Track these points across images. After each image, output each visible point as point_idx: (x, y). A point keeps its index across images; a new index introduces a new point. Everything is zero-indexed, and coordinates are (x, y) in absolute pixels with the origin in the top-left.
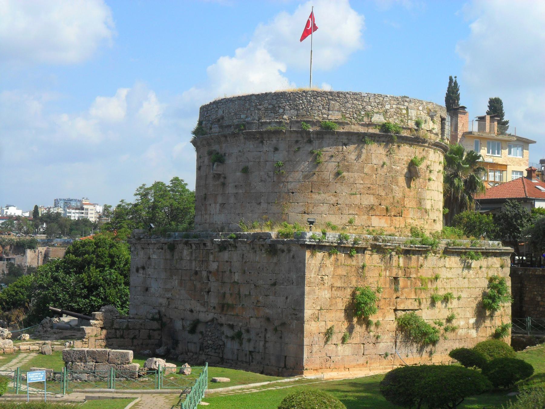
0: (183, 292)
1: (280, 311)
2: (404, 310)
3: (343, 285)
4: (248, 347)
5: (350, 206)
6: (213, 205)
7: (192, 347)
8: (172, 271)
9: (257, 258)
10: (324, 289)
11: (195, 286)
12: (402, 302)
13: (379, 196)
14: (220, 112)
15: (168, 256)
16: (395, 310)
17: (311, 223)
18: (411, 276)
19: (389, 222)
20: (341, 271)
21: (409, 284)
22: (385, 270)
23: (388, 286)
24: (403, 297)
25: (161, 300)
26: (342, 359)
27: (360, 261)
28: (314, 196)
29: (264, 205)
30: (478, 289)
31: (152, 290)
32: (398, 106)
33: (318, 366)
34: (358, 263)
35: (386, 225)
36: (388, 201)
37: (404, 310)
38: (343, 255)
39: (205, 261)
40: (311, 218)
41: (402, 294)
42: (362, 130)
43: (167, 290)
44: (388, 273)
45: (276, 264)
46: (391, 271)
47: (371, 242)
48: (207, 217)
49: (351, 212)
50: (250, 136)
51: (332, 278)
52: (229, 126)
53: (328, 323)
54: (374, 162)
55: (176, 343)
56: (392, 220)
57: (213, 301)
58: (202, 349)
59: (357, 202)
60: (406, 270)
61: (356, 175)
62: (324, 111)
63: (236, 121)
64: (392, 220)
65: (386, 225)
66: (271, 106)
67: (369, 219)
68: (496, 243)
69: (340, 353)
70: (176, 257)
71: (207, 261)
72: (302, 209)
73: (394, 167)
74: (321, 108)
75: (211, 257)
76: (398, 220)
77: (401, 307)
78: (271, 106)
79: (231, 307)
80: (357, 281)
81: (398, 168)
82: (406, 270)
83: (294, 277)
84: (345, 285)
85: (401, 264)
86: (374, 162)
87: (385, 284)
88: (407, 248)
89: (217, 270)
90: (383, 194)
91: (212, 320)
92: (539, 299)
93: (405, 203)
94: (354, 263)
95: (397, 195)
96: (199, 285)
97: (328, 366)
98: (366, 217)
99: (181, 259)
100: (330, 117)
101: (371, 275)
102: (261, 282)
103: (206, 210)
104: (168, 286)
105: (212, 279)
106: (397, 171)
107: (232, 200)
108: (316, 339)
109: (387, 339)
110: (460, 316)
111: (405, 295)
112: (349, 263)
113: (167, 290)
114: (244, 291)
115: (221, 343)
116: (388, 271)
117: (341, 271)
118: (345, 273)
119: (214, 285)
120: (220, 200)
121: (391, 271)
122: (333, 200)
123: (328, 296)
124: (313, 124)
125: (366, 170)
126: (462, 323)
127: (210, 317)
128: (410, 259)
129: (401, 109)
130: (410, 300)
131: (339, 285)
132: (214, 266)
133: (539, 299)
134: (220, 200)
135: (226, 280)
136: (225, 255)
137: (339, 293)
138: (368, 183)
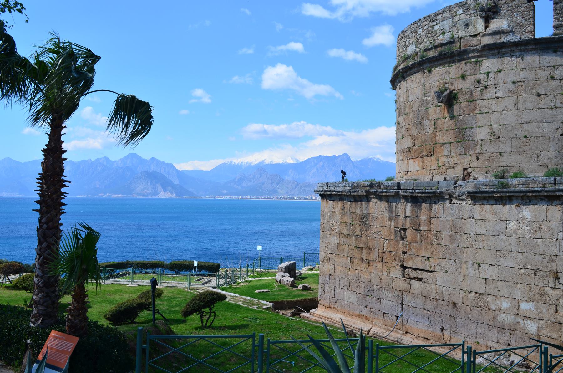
2: (415, 269)
3: (348, 233)
10: (334, 235)
13: (413, 137)
16: (404, 267)
18: (421, 228)
19: (421, 164)
20: (347, 219)
21: (419, 237)
22: (390, 219)
24: (411, 253)
26: (347, 304)
27: (364, 209)
30: (540, 258)
32: (431, 24)
34: (362, 211)
36: (420, 140)
37: (415, 269)
38: (349, 203)
41: (410, 249)
44: (393, 224)
47: (367, 189)
51: (340, 225)
53: (336, 267)
56: (423, 162)
64: (423, 162)
69: (346, 298)
73: (425, 98)
76: (429, 160)
80: (361, 230)
81: (429, 98)
84: (351, 233)
85: (408, 214)
87: (390, 235)
88: (407, 194)
93: (437, 139)
94: (358, 211)
95: (428, 130)
97: (335, 306)
101: (375, 224)
108: (327, 279)
109: (392, 297)
110: (501, 293)
112: (354, 211)
116: (393, 221)
118: (349, 221)
123: (337, 241)
128: (420, 208)
129: (433, 26)
130: (421, 258)
137: (345, 240)
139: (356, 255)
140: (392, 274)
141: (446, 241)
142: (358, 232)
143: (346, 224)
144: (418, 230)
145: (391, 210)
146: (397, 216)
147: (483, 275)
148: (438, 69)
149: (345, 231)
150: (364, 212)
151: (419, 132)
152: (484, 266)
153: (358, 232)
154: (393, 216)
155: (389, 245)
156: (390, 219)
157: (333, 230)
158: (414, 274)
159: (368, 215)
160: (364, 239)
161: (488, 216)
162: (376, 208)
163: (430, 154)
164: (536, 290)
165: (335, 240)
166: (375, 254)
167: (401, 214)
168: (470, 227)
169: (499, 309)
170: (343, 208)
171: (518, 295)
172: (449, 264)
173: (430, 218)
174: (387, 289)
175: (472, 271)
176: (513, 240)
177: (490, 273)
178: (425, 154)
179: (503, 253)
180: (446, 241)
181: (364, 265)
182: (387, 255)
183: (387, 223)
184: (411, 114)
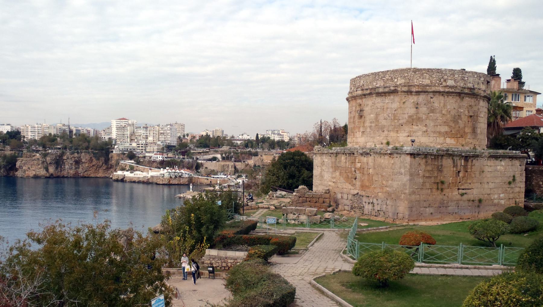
0: (342, 179)
1: (394, 189)
2: (463, 189)
4: (377, 208)
5: (434, 132)
6: (358, 133)
7: (346, 208)
8: (336, 168)
9: (382, 161)
11: (348, 176)
12: (462, 185)
14: (362, 82)
15: (333, 160)
17: (413, 142)
20: (429, 168)
23: (455, 176)
25: (330, 183)
28: (414, 127)
29: (386, 132)
31: (325, 178)
33: (415, 219)
35: (454, 143)
37: (463, 189)
39: (354, 163)
40: (413, 138)
42: (442, 90)
43: (334, 178)
45: (393, 164)
46: (457, 168)
48: (355, 139)
49: (434, 135)
50: (379, 94)
52: (367, 89)
54: (449, 107)
55: (337, 205)
56: (458, 140)
57: (358, 183)
58: (352, 209)
59: (438, 130)
60: (465, 167)
61: (438, 115)
62: (420, 80)
63: (370, 87)
64: (458, 140)
65: (454, 143)
66: (390, 78)
67: (445, 139)
68: (518, 152)
70: (338, 160)
71: (355, 162)
72: (407, 134)
74: (418, 78)
75: (357, 161)
77: (462, 187)
78: (390, 78)
79: (368, 187)
80: (437, 174)
82: (465, 167)
83: (403, 171)
85: (463, 164)
86: (449, 107)
89: (360, 167)
90: (453, 125)
91: (358, 193)
92: (541, 183)
94: (436, 163)
96: (350, 175)
98: (443, 138)
99: (340, 161)
100: (423, 83)
102: (384, 174)
103: (354, 135)
104: (334, 176)
105: (357, 172)
106: (461, 112)
107: (368, 130)
111: (464, 181)
113: (334, 178)
114: (375, 178)
115: (362, 206)
117: (429, 168)
118: (431, 169)
119: (358, 175)
120: (362, 129)
121: (457, 168)
122: (425, 129)
124: (414, 86)
125: (443, 112)
126: (496, 196)
127: (356, 192)
131: (428, 175)
132: (358, 165)
133: (541, 183)
134: (362, 129)
135: (365, 173)
136: (364, 159)
137: (428, 180)
138: (444, 119)
139: (434, 187)
140: (454, 194)
141: (477, 175)
142: (436, 174)
143: (429, 171)
144: (467, 171)
145: (454, 163)
146: (457, 165)
147: (490, 187)
148: (467, 98)
149: (427, 175)
150: (440, 164)
151: (455, 125)
152: (490, 184)
153: (436, 174)
154: (455, 166)
155: (452, 180)
156: (454, 167)
157: (419, 175)
158: (464, 191)
159: (442, 165)
160: (439, 178)
161: (492, 164)
162: (447, 162)
163: (462, 136)
164: (504, 189)
165: (421, 180)
166: (446, 185)
167: (459, 164)
168: (487, 169)
169: (494, 199)
170: (427, 162)
171: (500, 192)
172: (478, 185)
173: (472, 166)
174: (452, 201)
175: (486, 186)
176: (499, 173)
177: (492, 185)
178: (458, 136)
179: (496, 177)
180: (477, 175)
181: (439, 191)
182: (451, 185)
183: (452, 169)
184: (448, 116)
